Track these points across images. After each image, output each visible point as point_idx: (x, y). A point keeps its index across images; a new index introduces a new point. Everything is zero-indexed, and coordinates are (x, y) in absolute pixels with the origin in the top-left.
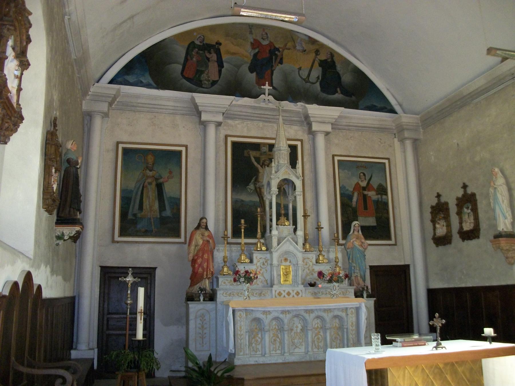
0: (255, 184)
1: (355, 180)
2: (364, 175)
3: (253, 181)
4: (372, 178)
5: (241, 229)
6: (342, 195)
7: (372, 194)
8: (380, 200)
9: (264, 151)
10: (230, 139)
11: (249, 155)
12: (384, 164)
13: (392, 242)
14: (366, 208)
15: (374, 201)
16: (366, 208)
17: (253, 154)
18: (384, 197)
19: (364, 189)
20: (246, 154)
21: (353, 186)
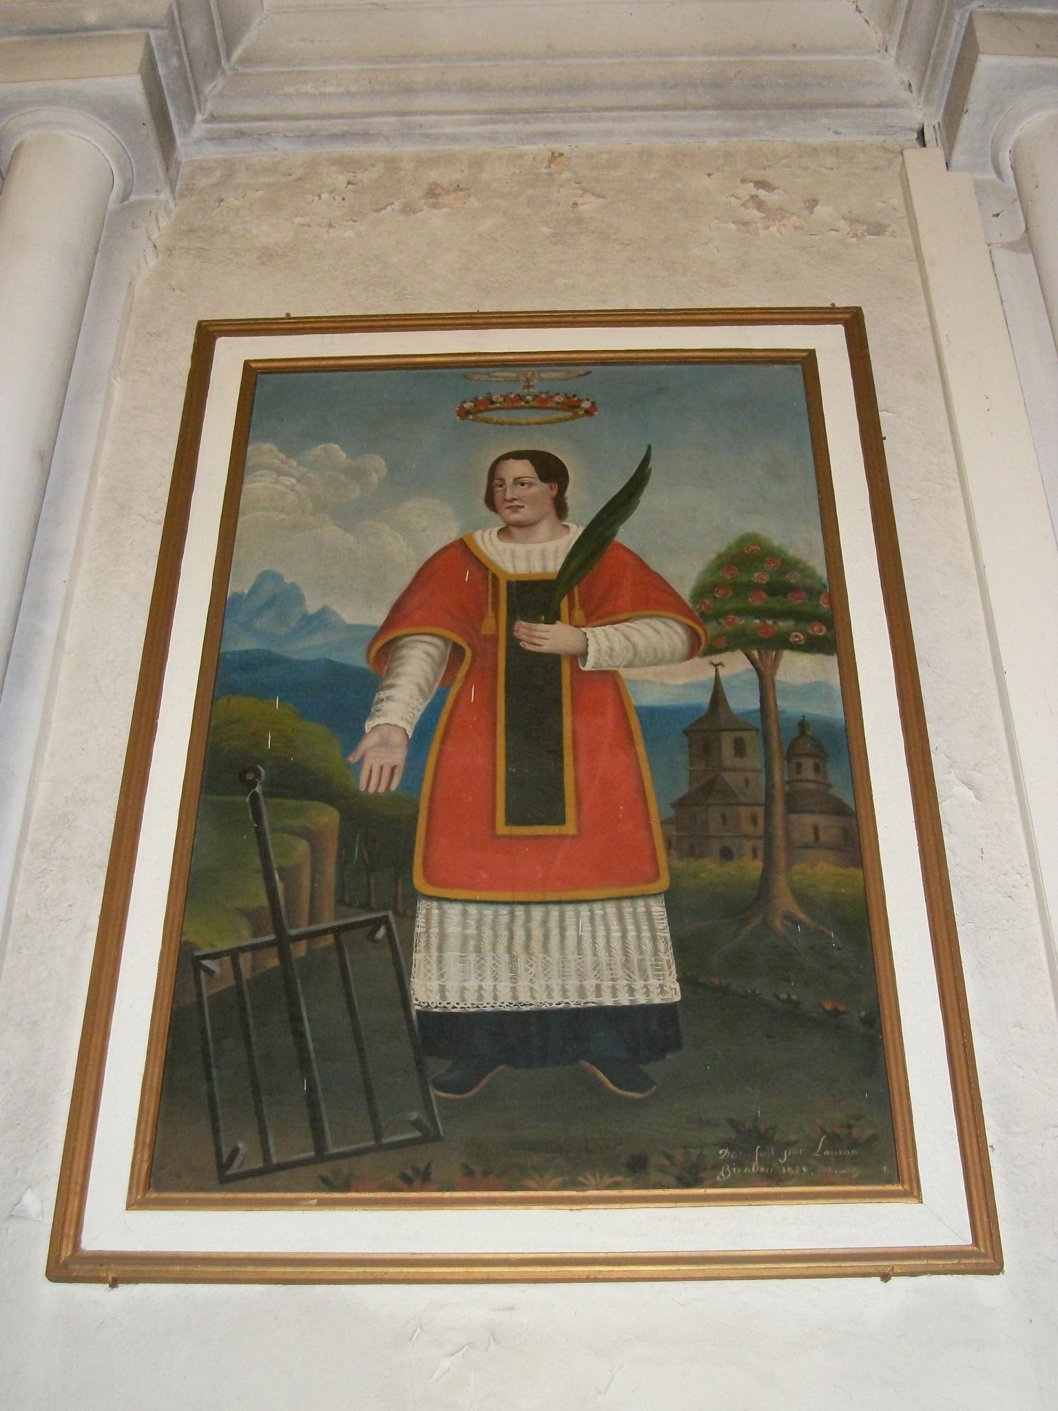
1: (428, 527)
2: (550, 470)
4: (648, 499)
6: (222, 674)
7: (645, 659)
8: (743, 701)
12: (807, 362)
13: (935, 1212)
14: (537, 798)
15: (650, 715)
16: (537, 798)
18: (799, 670)
19: (535, 599)
21: (402, 581)
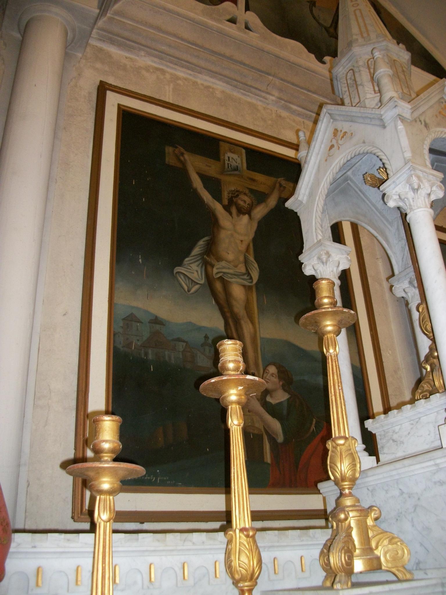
0: (206, 265)
3: (197, 251)
5: (223, 413)
9: (234, 164)
10: (113, 101)
11: (184, 163)
17: (195, 165)
20: (170, 159)
